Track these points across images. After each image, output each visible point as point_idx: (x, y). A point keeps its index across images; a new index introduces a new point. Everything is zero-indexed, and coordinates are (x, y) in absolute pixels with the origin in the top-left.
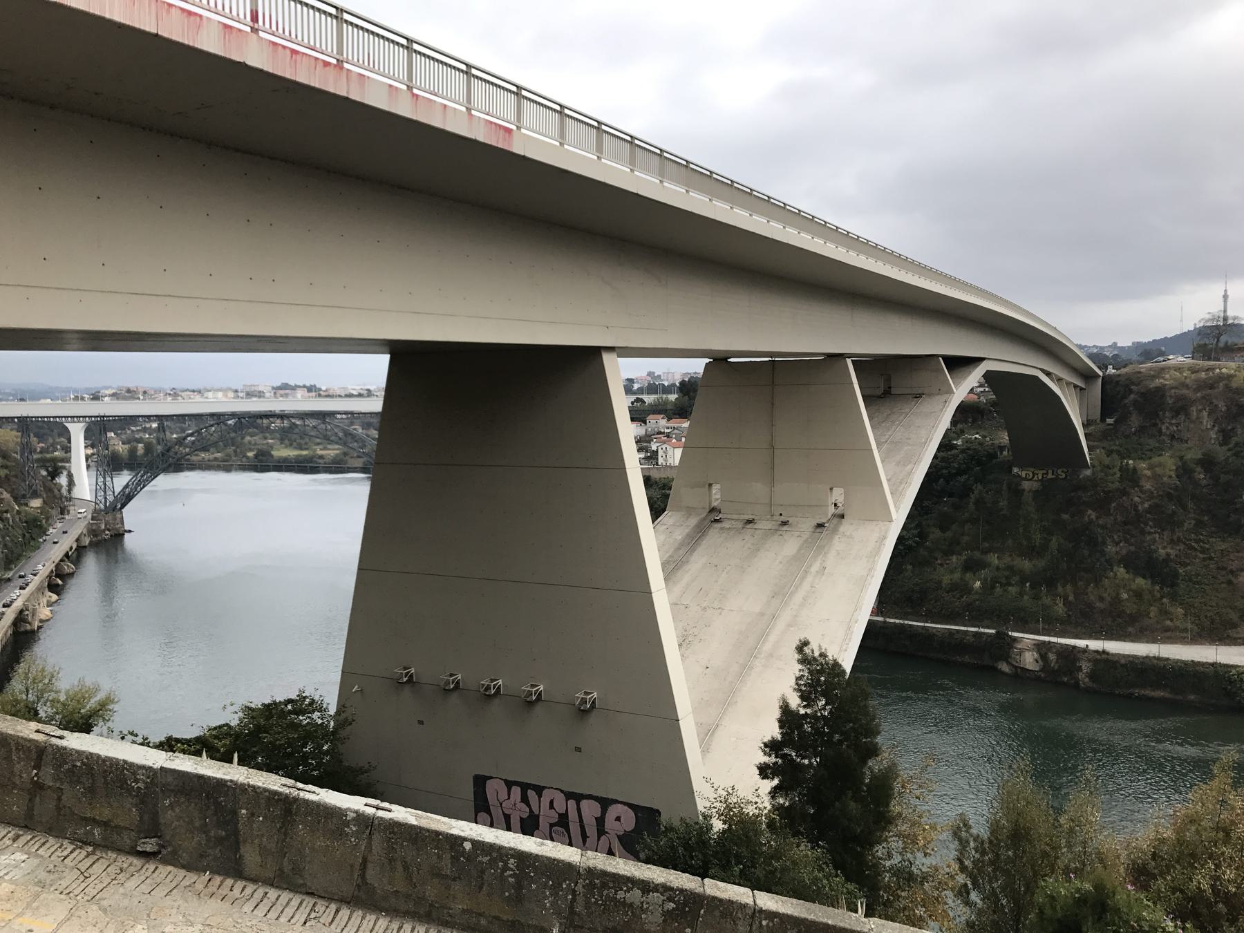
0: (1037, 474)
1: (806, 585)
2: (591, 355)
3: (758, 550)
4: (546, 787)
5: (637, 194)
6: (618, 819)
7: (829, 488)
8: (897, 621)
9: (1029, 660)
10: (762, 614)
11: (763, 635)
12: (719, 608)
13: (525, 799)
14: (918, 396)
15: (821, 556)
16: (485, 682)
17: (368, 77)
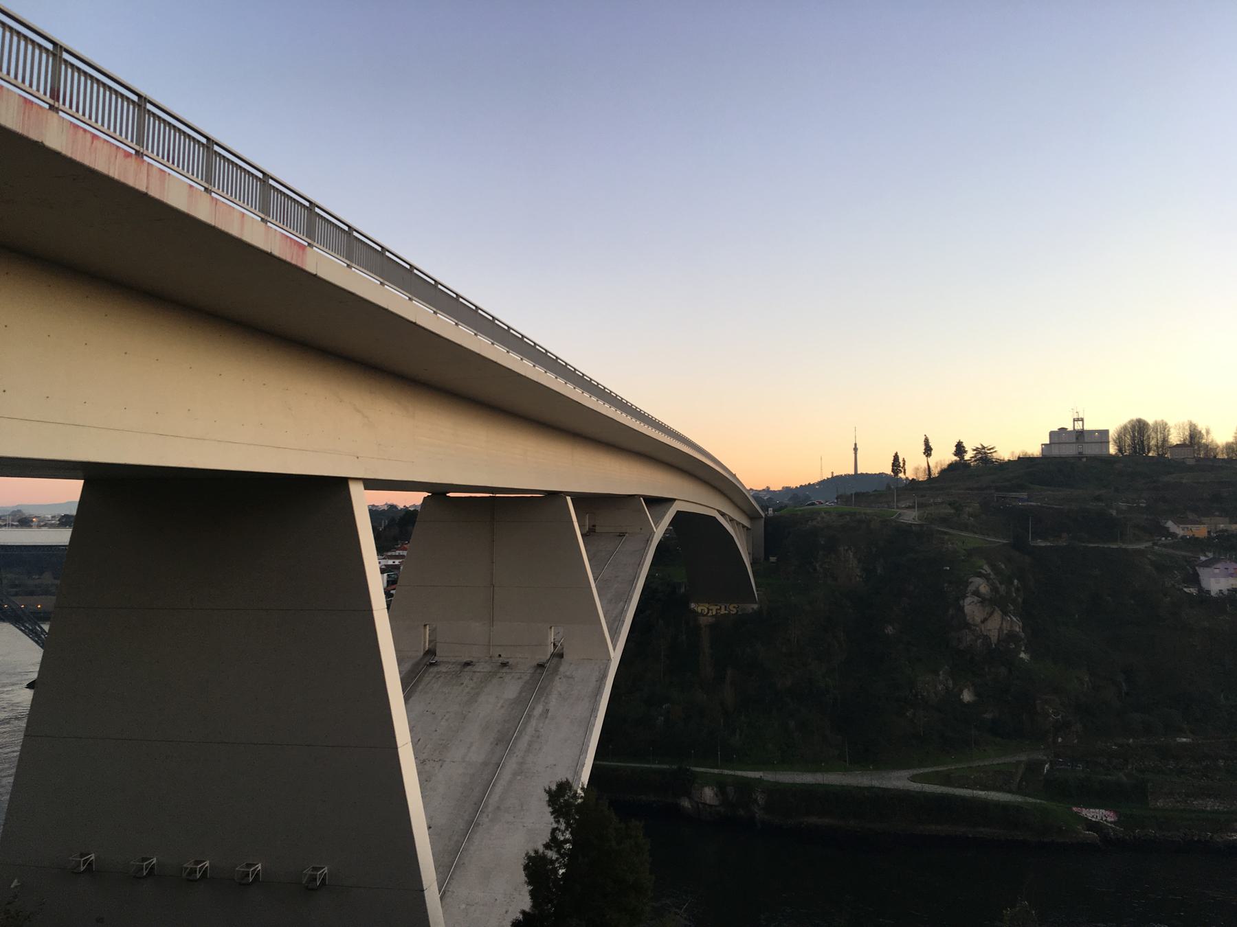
0: (712, 610)
1: (530, 730)
3: (478, 694)
5: (415, 323)
7: (549, 627)
8: (605, 763)
9: (709, 794)
10: (485, 764)
11: (488, 785)
12: (440, 760)
14: (622, 535)
15: (544, 698)
16: (189, 865)
17: (169, 174)
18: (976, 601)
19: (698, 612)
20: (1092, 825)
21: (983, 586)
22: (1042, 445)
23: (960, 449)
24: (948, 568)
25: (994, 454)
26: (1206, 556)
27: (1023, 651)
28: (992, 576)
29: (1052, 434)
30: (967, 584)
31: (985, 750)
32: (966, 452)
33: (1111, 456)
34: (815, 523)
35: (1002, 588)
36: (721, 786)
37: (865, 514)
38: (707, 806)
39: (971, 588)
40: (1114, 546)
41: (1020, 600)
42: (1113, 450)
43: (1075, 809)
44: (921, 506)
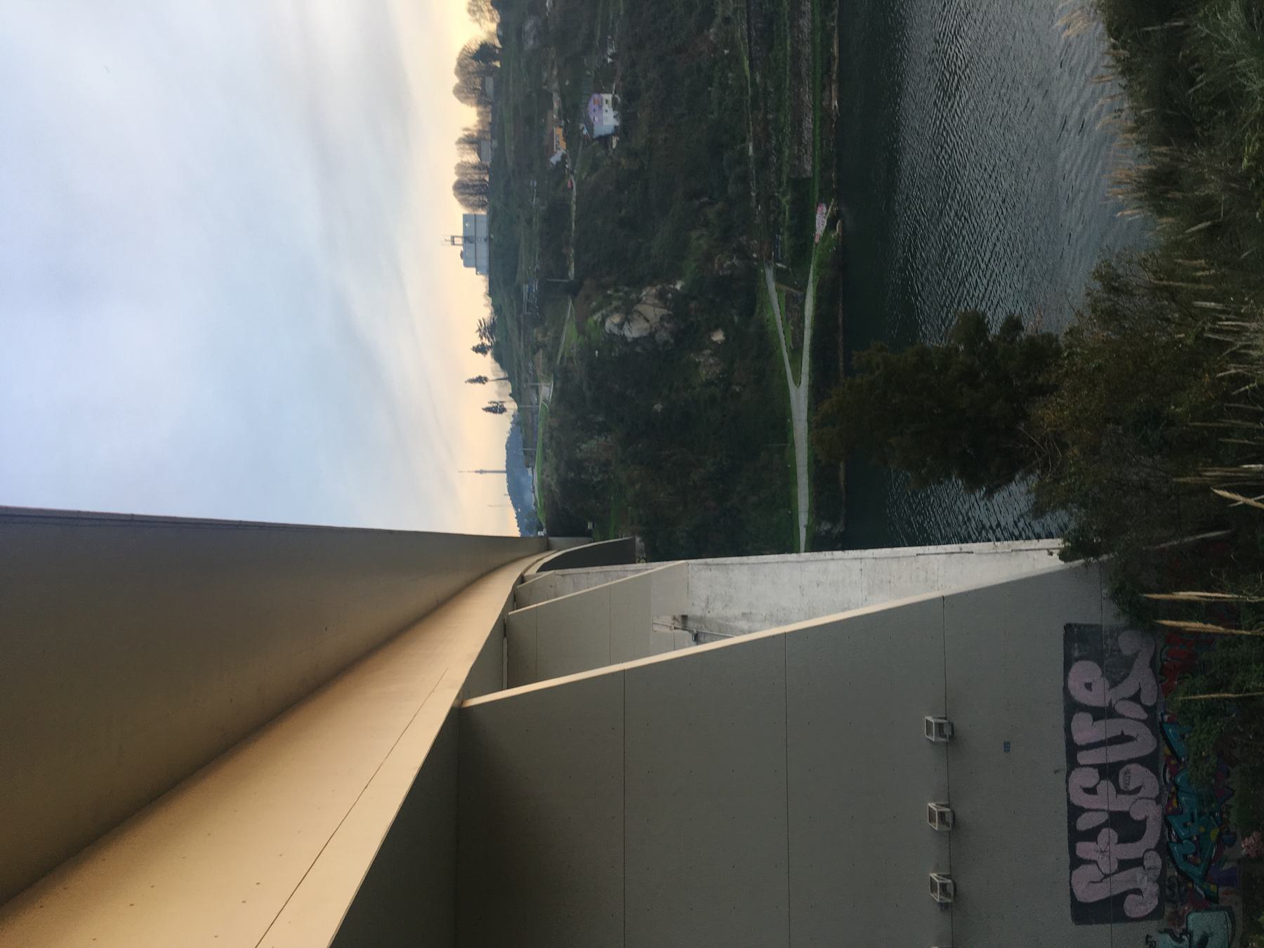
6: (1088, 686)
15: (731, 624)
18: (628, 327)
20: (831, 225)
21: (613, 320)
22: (477, 274)
23: (480, 349)
24: (597, 352)
25: (486, 321)
26: (583, 128)
27: (674, 285)
28: (604, 312)
29: (466, 265)
30: (612, 335)
31: (768, 321)
32: (483, 344)
33: (488, 213)
34: (553, 483)
35: (615, 303)
37: (543, 435)
39: (616, 331)
40: (574, 207)
41: (626, 289)
42: (482, 213)
43: (817, 240)
44: (536, 380)
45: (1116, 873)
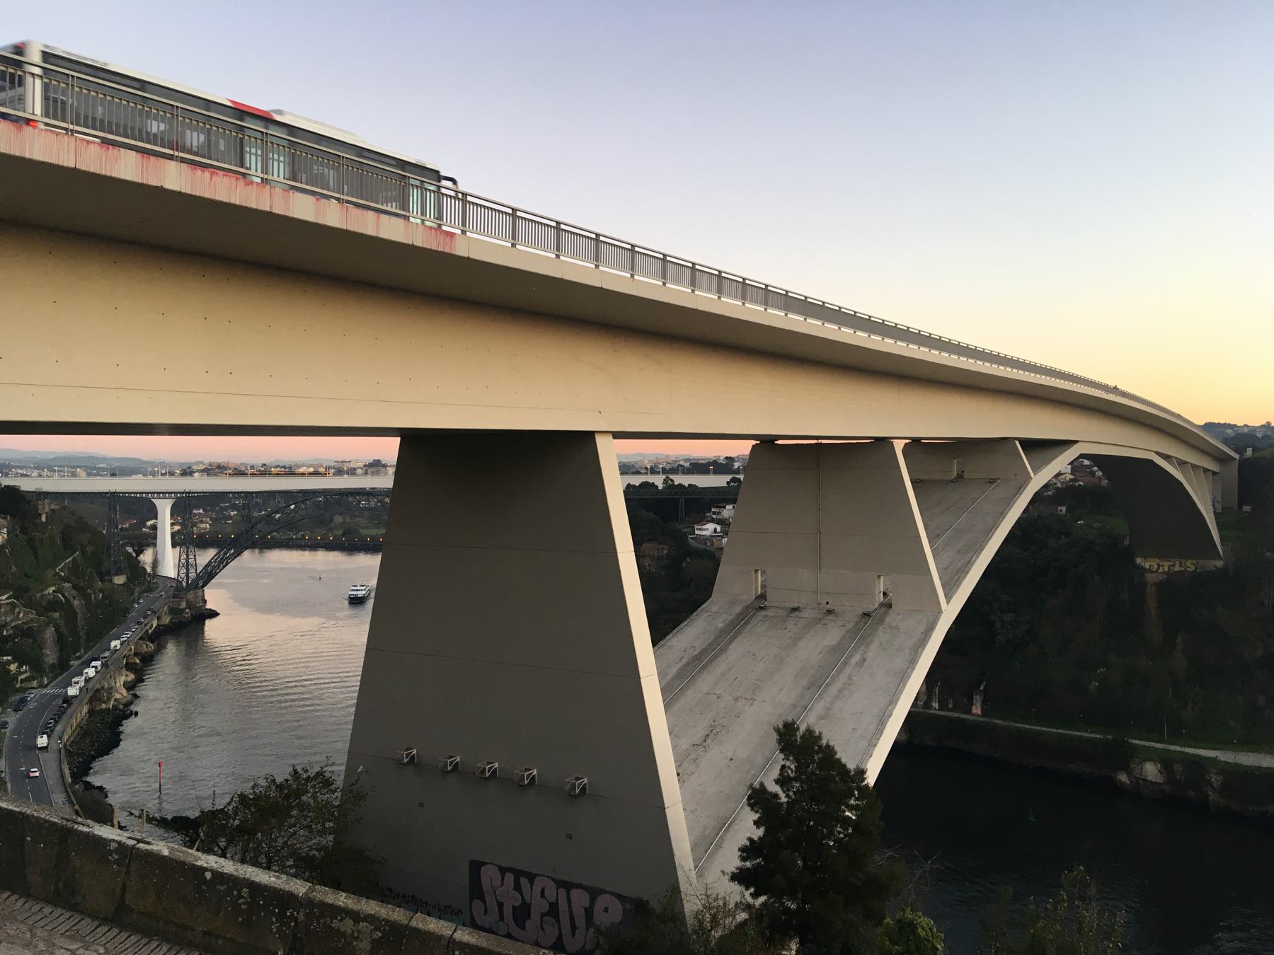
0: (1163, 566)
1: (843, 678)
2: (585, 440)
3: (799, 639)
4: (486, 863)
6: (606, 910)
7: (876, 576)
9: (1151, 771)
13: (518, 887)
14: (992, 481)
15: (863, 646)
19: (1145, 569)
36: (1166, 762)
38: (1148, 783)
45: (496, 899)
